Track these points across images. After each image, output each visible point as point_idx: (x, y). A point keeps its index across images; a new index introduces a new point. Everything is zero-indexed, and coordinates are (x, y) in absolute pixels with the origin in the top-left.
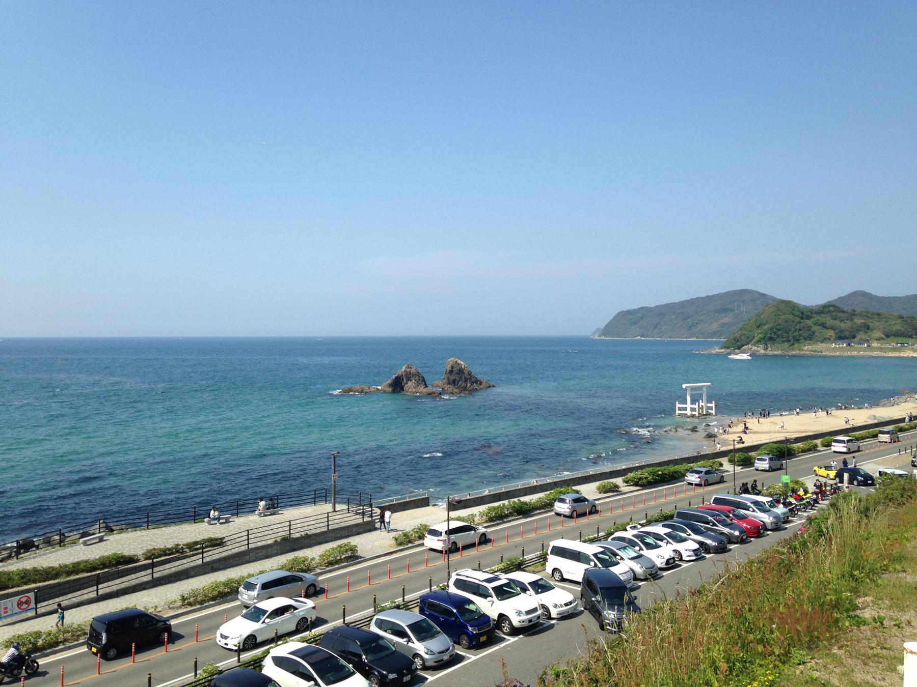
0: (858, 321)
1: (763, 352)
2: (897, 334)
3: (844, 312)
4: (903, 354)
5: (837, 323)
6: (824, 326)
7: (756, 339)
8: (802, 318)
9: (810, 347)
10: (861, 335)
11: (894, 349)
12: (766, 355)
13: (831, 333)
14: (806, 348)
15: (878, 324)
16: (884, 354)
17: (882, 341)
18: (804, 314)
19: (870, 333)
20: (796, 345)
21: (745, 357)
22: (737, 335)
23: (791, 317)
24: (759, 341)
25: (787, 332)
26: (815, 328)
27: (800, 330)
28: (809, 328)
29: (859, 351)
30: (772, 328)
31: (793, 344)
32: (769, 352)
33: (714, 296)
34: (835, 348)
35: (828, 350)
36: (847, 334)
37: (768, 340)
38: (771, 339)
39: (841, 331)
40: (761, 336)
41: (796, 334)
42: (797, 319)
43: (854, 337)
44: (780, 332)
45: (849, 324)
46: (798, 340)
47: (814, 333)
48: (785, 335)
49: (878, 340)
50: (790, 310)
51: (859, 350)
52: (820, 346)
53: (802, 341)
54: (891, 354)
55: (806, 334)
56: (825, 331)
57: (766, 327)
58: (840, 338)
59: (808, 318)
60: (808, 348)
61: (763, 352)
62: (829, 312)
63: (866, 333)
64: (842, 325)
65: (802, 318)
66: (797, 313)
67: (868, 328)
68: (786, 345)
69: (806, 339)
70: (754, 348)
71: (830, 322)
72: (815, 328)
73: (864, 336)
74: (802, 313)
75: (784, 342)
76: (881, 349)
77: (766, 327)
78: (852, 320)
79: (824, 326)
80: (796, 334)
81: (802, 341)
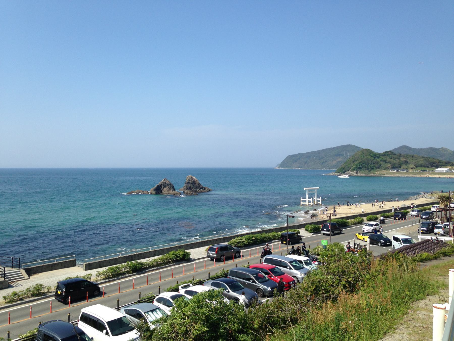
0: (402, 159)
1: (355, 174)
2: (421, 166)
3: (395, 155)
4: (424, 176)
5: (392, 160)
6: (385, 161)
7: (352, 168)
8: (375, 158)
9: (379, 172)
10: (404, 166)
11: (420, 173)
12: (357, 176)
13: (389, 165)
14: (376, 173)
15: (412, 161)
16: (415, 176)
17: (414, 169)
18: (376, 156)
19: (408, 165)
20: (372, 171)
21: (346, 177)
22: (343, 166)
23: (370, 157)
24: (354, 169)
25: (368, 164)
26: (381, 163)
27: (374, 163)
28: (379, 162)
29: (402, 174)
30: (360, 163)
31: (370, 171)
32: (358, 175)
33: (334, 148)
34: (391, 172)
35: (388, 173)
36: (397, 165)
37: (358, 168)
38: (359, 168)
39: (394, 164)
40: (354, 166)
41: (372, 165)
42: (373, 158)
43: (400, 167)
44: (364, 165)
45: (398, 160)
46: (373, 169)
47: (381, 165)
48: (366, 166)
49: (412, 168)
50: (369, 153)
51: (402, 174)
52: (383, 172)
53: (375, 169)
54: (418, 176)
55: (377, 166)
56: (386, 164)
57: (357, 162)
58: (394, 167)
59: (378, 157)
60: (377, 173)
61: (355, 174)
62: (388, 155)
63: (406, 165)
64: (395, 161)
65: (375, 158)
66: (373, 155)
67: (407, 163)
68: (367, 171)
69: (376, 168)
70: (351, 173)
71: (388, 159)
72: (381, 163)
73: (405, 167)
74: (375, 155)
75: (366, 169)
76: (413, 173)
77: (357, 162)
78: (399, 159)
79: (385, 161)
80: (372, 165)
81: (375, 169)
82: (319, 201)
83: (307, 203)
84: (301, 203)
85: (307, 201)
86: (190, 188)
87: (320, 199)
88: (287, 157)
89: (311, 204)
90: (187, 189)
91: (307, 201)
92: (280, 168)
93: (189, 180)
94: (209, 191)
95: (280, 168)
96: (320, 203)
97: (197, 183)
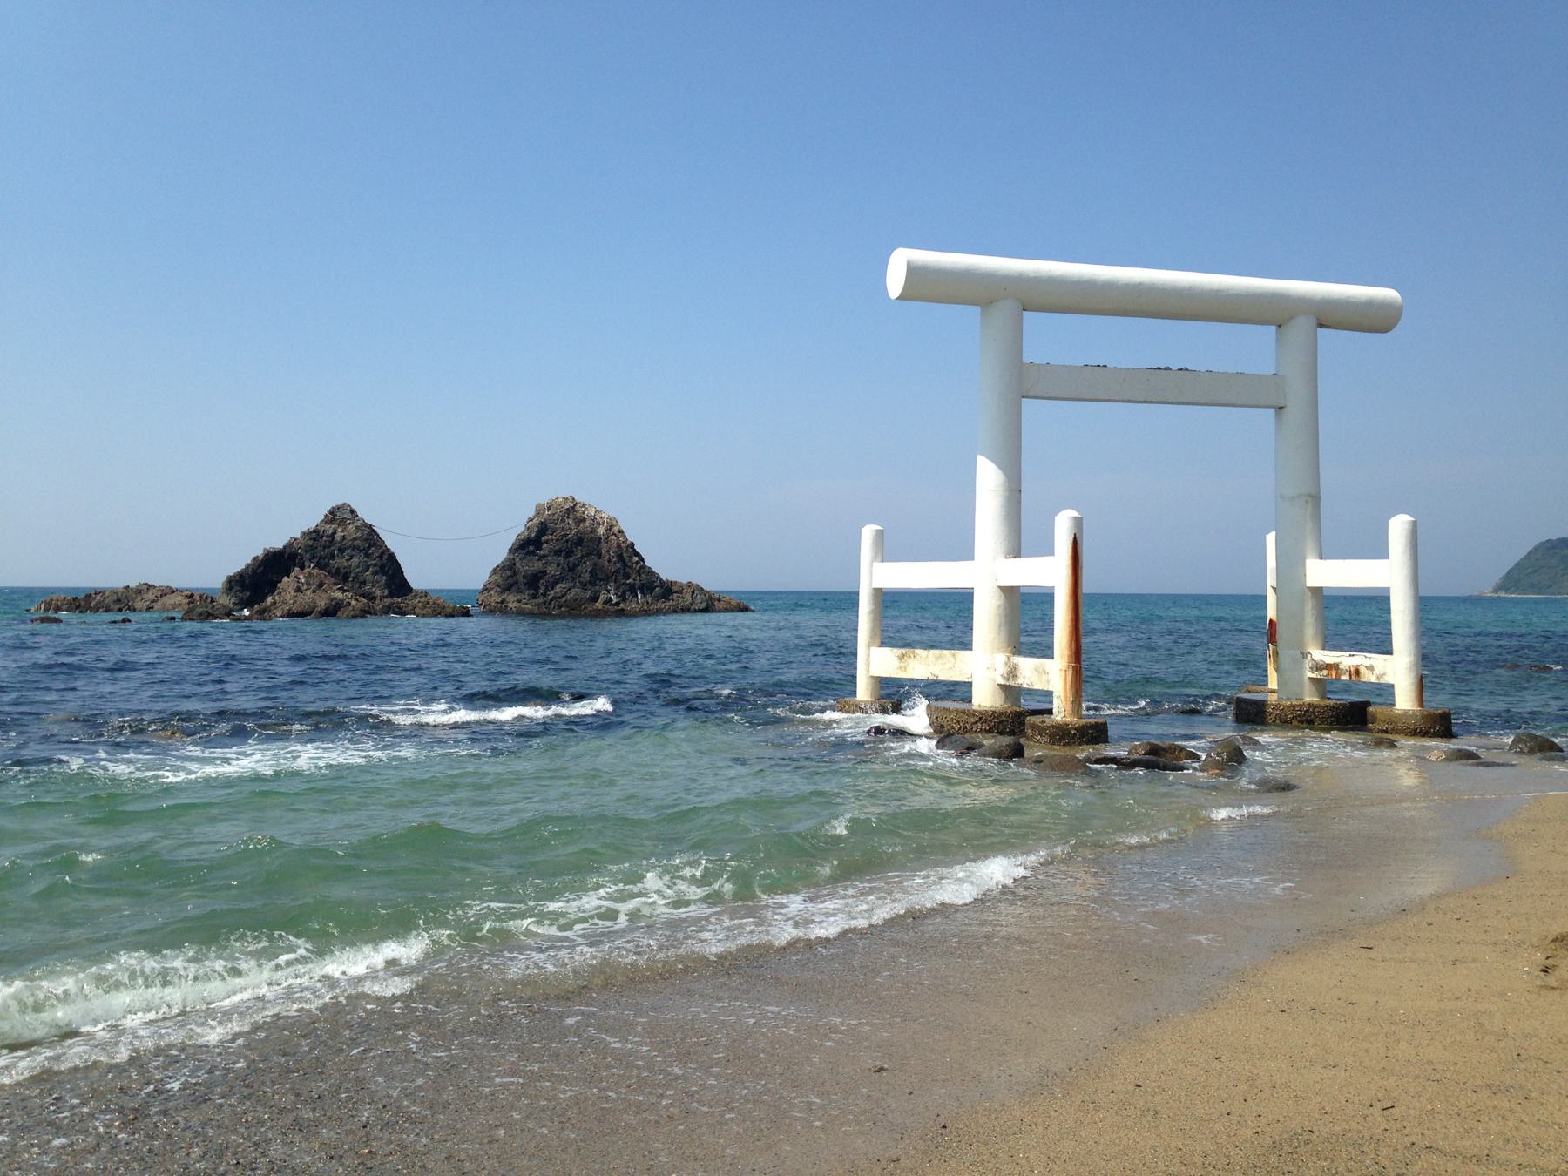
82: (1358, 619)
83: (983, 669)
84: (876, 662)
85: (986, 617)
86: (533, 581)
87: (1387, 574)
88: (1536, 549)
89: (1050, 675)
90: (507, 588)
91: (986, 617)
92: (1503, 594)
93: (543, 529)
94: (705, 610)
95: (1503, 594)
96: (1395, 671)
97: (608, 551)
